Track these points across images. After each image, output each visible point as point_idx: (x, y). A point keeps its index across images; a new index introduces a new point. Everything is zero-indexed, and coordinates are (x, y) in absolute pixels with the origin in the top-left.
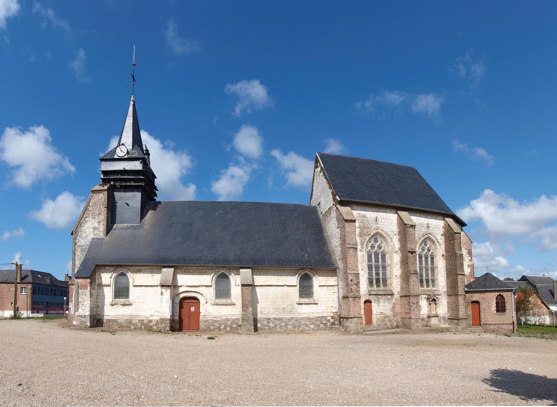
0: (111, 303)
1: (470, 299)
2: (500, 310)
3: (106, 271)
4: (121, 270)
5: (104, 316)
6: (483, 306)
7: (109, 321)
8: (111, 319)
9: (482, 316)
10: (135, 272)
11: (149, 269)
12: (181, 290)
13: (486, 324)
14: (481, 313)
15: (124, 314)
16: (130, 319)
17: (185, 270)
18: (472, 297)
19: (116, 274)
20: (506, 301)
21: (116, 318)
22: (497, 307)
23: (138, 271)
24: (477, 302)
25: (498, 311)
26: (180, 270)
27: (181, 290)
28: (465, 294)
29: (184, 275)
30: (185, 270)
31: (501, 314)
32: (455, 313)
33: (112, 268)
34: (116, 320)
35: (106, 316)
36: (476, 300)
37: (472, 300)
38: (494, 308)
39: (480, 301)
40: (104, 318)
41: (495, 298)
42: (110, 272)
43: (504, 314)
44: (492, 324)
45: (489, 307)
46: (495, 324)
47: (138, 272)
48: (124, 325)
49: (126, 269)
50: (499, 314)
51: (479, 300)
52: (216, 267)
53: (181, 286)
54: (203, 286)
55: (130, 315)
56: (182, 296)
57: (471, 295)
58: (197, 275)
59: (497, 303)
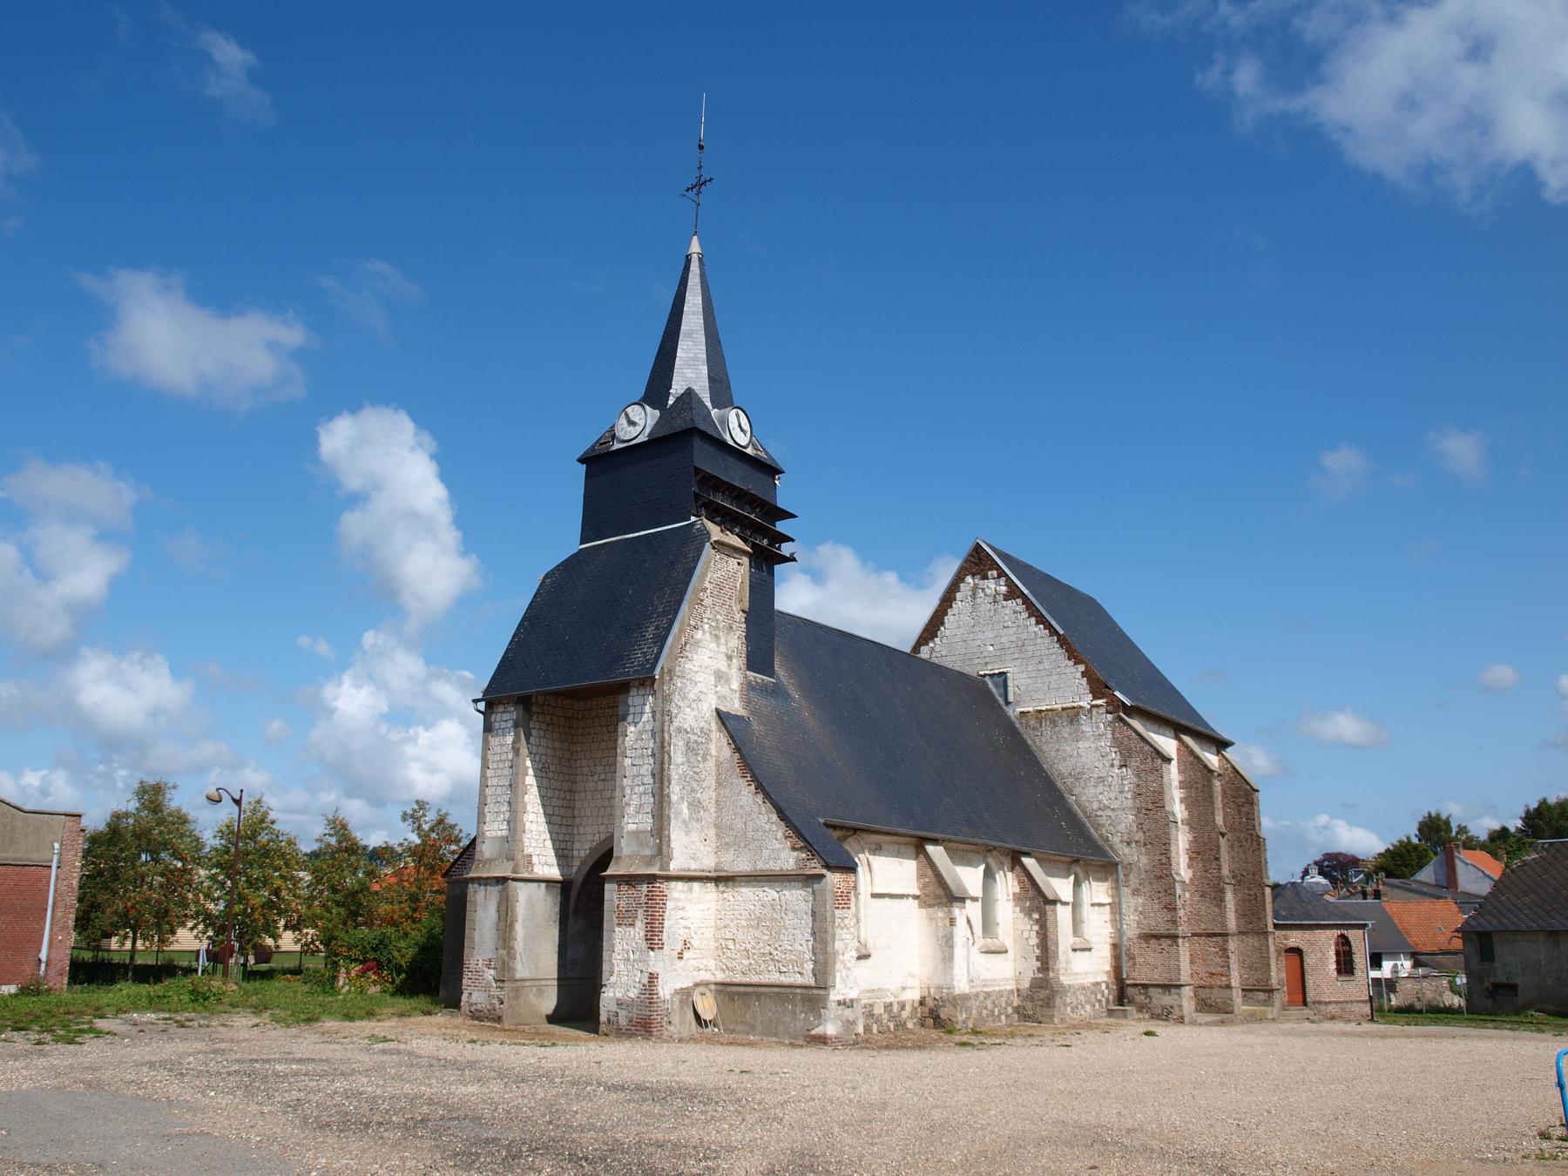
1: (1282, 943)
2: (1343, 970)
6: (1310, 961)
9: (1310, 982)
13: (1320, 1003)
14: (1307, 977)
18: (1286, 939)
20: (1354, 949)
22: (1338, 962)
24: (1298, 951)
25: (1339, 971)
28: (1274, 930)
31: (1347, 978)
32: (1258, 975)
36: (1295, 945)
37: (1286, 945)
38: (1332, 966)
39: (1304, 949)
41: (1332, 942)
43: (1352, 978)
44: (1330, 1002)
45: (1323, 961)
46: (1336, 1003)
50: (1343, 978)
51: (1301, 947)
57: (1283, 933)
59: (1338, 953)
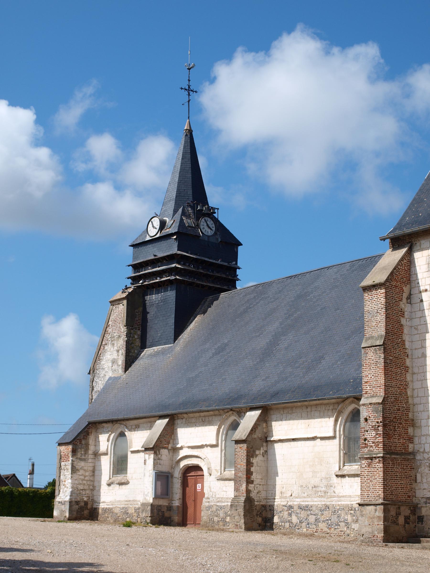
0: (108, 481)
3: (104, 430)
4: (120, 428)
5: (100, 503)
7: (105, 510)
8: (106, 508)
10: (134, 429)
11: (148, 423)
12: (182, 453)
15: (121, 500)
16: (126, 506)
17: (186, 419)
19: (114, 434)
21: (111, 506)
23: (136, 428)
26: (181, 421)
27: (182, 453)
29: (186, 429)
30: (186, 419)
33: (109, 425)
34: (112, 509)
35: (102, 502)
40: (100, 507)
42: (107, 432)
47: (136, 429)
48: (120, 518)
49: (122, 426)
52: (223, 410)
53: (181, 448)
54: (207, 446)
55: (127, 501)
56: (183, 464)
58: (200, 426)
